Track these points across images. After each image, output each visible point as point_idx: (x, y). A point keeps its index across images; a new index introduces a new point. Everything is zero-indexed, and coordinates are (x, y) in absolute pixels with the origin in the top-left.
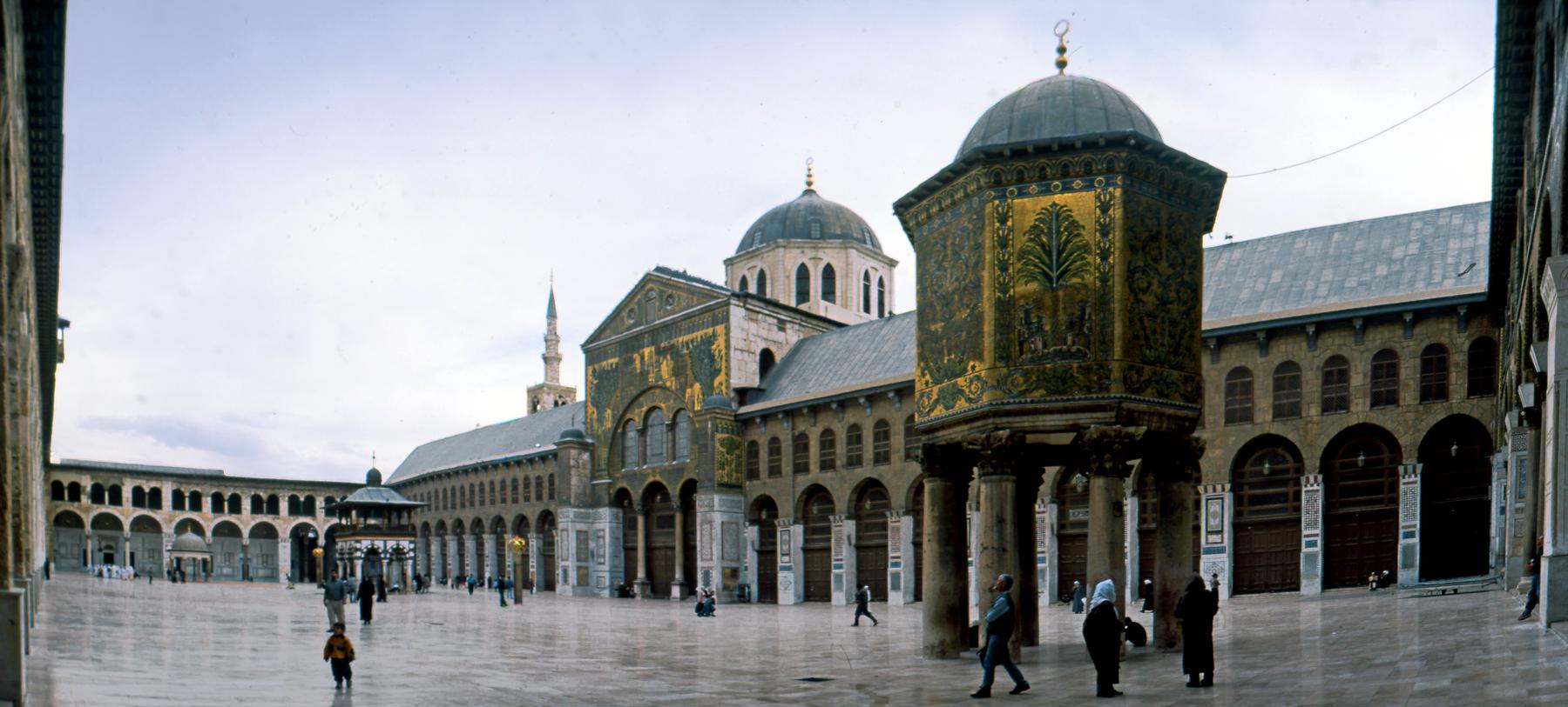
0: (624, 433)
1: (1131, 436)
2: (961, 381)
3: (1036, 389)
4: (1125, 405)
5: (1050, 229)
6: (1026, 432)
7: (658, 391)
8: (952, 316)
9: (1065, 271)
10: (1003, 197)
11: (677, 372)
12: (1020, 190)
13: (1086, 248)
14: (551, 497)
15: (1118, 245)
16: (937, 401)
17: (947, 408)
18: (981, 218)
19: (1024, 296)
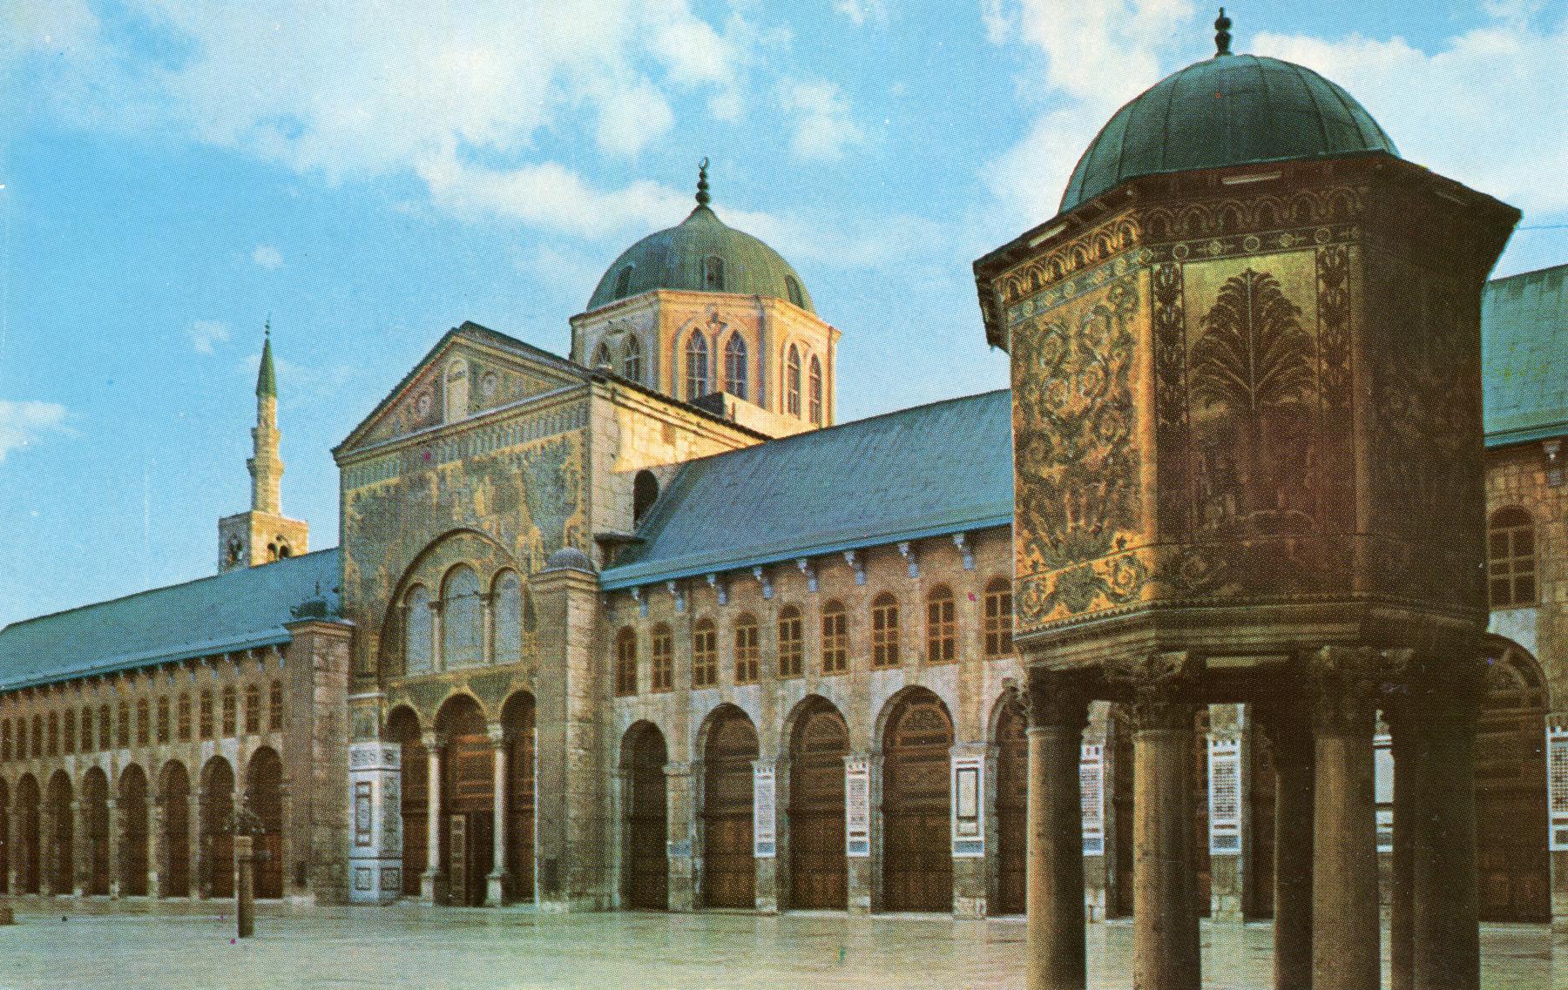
0: (406, 611)
1: (1387, 665)
2: (1098, 565)
3: (1229, 580)
4: (1379, 612)
5: (1243, 314)
6: (1209, 652)
7: (464, 536)
8: (1080, 453)
9: (1271, 384)
10: (1167, 258)
11: (502, 504)
12: (1193, 247)
13: (1303, 344)
14: (276, 724)
15: (1355, 339)
16: (1053, 597)
17: (1073, 610)
18: (1130, 292)
19: (1204, 425)
